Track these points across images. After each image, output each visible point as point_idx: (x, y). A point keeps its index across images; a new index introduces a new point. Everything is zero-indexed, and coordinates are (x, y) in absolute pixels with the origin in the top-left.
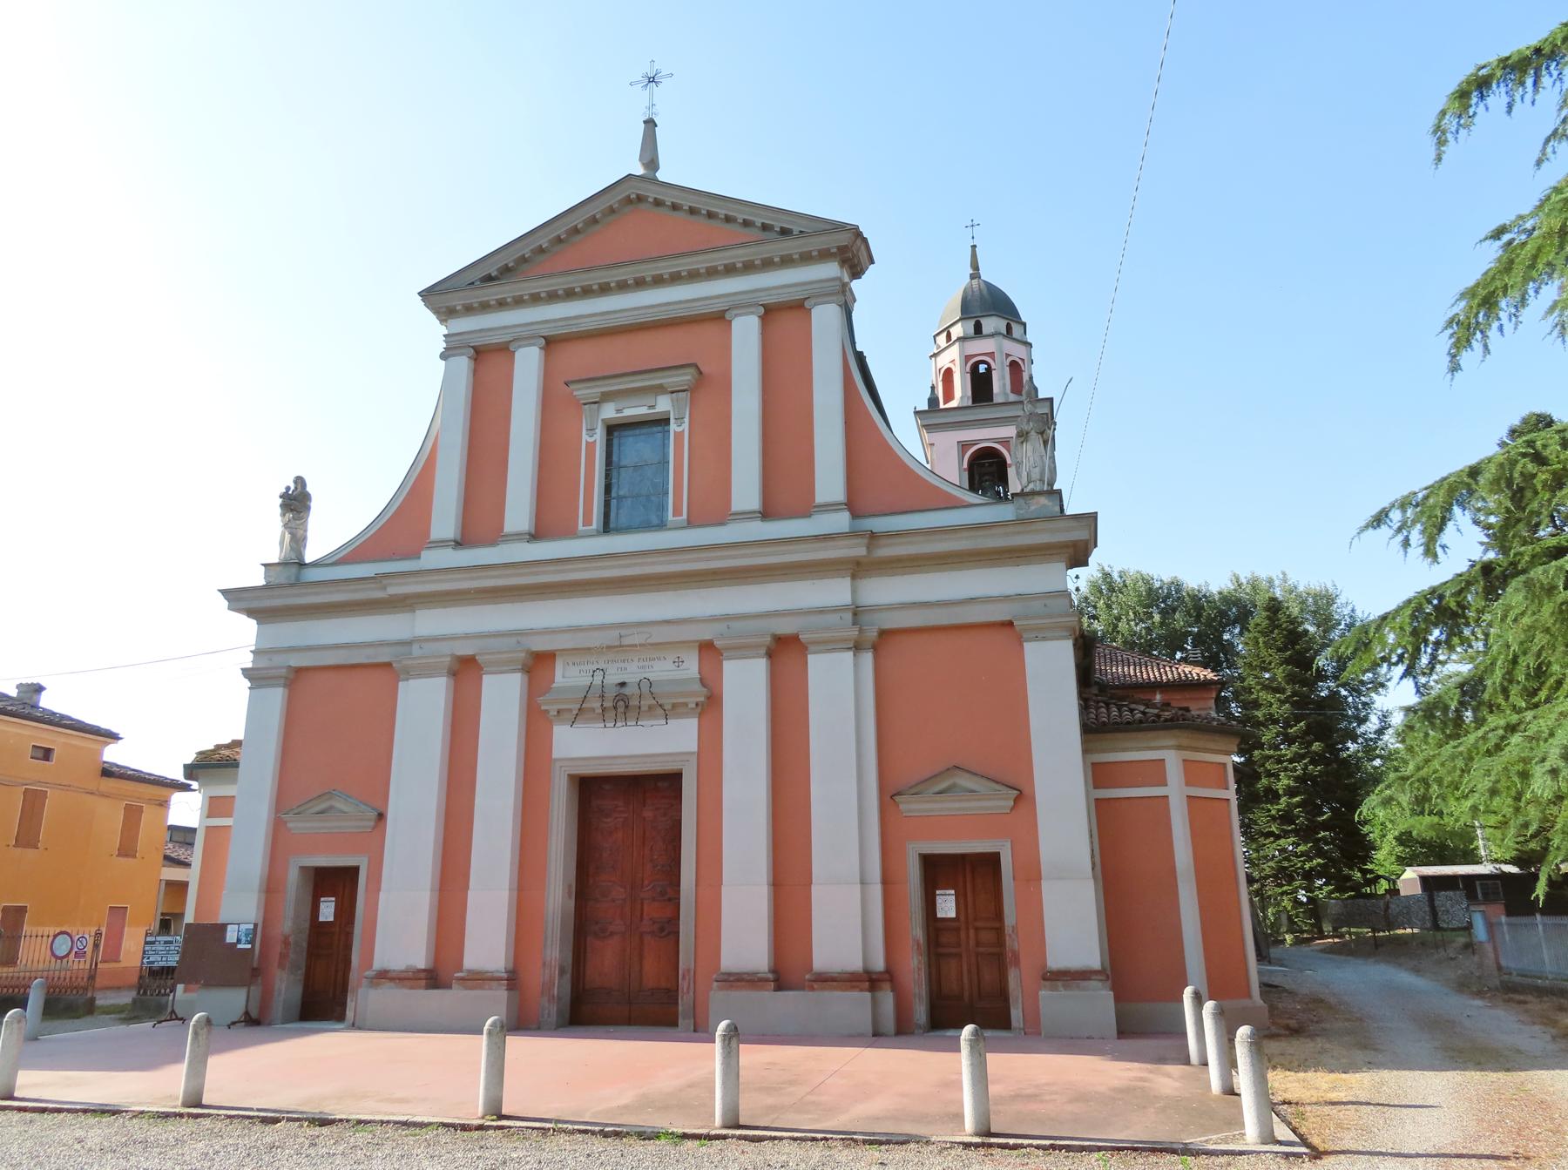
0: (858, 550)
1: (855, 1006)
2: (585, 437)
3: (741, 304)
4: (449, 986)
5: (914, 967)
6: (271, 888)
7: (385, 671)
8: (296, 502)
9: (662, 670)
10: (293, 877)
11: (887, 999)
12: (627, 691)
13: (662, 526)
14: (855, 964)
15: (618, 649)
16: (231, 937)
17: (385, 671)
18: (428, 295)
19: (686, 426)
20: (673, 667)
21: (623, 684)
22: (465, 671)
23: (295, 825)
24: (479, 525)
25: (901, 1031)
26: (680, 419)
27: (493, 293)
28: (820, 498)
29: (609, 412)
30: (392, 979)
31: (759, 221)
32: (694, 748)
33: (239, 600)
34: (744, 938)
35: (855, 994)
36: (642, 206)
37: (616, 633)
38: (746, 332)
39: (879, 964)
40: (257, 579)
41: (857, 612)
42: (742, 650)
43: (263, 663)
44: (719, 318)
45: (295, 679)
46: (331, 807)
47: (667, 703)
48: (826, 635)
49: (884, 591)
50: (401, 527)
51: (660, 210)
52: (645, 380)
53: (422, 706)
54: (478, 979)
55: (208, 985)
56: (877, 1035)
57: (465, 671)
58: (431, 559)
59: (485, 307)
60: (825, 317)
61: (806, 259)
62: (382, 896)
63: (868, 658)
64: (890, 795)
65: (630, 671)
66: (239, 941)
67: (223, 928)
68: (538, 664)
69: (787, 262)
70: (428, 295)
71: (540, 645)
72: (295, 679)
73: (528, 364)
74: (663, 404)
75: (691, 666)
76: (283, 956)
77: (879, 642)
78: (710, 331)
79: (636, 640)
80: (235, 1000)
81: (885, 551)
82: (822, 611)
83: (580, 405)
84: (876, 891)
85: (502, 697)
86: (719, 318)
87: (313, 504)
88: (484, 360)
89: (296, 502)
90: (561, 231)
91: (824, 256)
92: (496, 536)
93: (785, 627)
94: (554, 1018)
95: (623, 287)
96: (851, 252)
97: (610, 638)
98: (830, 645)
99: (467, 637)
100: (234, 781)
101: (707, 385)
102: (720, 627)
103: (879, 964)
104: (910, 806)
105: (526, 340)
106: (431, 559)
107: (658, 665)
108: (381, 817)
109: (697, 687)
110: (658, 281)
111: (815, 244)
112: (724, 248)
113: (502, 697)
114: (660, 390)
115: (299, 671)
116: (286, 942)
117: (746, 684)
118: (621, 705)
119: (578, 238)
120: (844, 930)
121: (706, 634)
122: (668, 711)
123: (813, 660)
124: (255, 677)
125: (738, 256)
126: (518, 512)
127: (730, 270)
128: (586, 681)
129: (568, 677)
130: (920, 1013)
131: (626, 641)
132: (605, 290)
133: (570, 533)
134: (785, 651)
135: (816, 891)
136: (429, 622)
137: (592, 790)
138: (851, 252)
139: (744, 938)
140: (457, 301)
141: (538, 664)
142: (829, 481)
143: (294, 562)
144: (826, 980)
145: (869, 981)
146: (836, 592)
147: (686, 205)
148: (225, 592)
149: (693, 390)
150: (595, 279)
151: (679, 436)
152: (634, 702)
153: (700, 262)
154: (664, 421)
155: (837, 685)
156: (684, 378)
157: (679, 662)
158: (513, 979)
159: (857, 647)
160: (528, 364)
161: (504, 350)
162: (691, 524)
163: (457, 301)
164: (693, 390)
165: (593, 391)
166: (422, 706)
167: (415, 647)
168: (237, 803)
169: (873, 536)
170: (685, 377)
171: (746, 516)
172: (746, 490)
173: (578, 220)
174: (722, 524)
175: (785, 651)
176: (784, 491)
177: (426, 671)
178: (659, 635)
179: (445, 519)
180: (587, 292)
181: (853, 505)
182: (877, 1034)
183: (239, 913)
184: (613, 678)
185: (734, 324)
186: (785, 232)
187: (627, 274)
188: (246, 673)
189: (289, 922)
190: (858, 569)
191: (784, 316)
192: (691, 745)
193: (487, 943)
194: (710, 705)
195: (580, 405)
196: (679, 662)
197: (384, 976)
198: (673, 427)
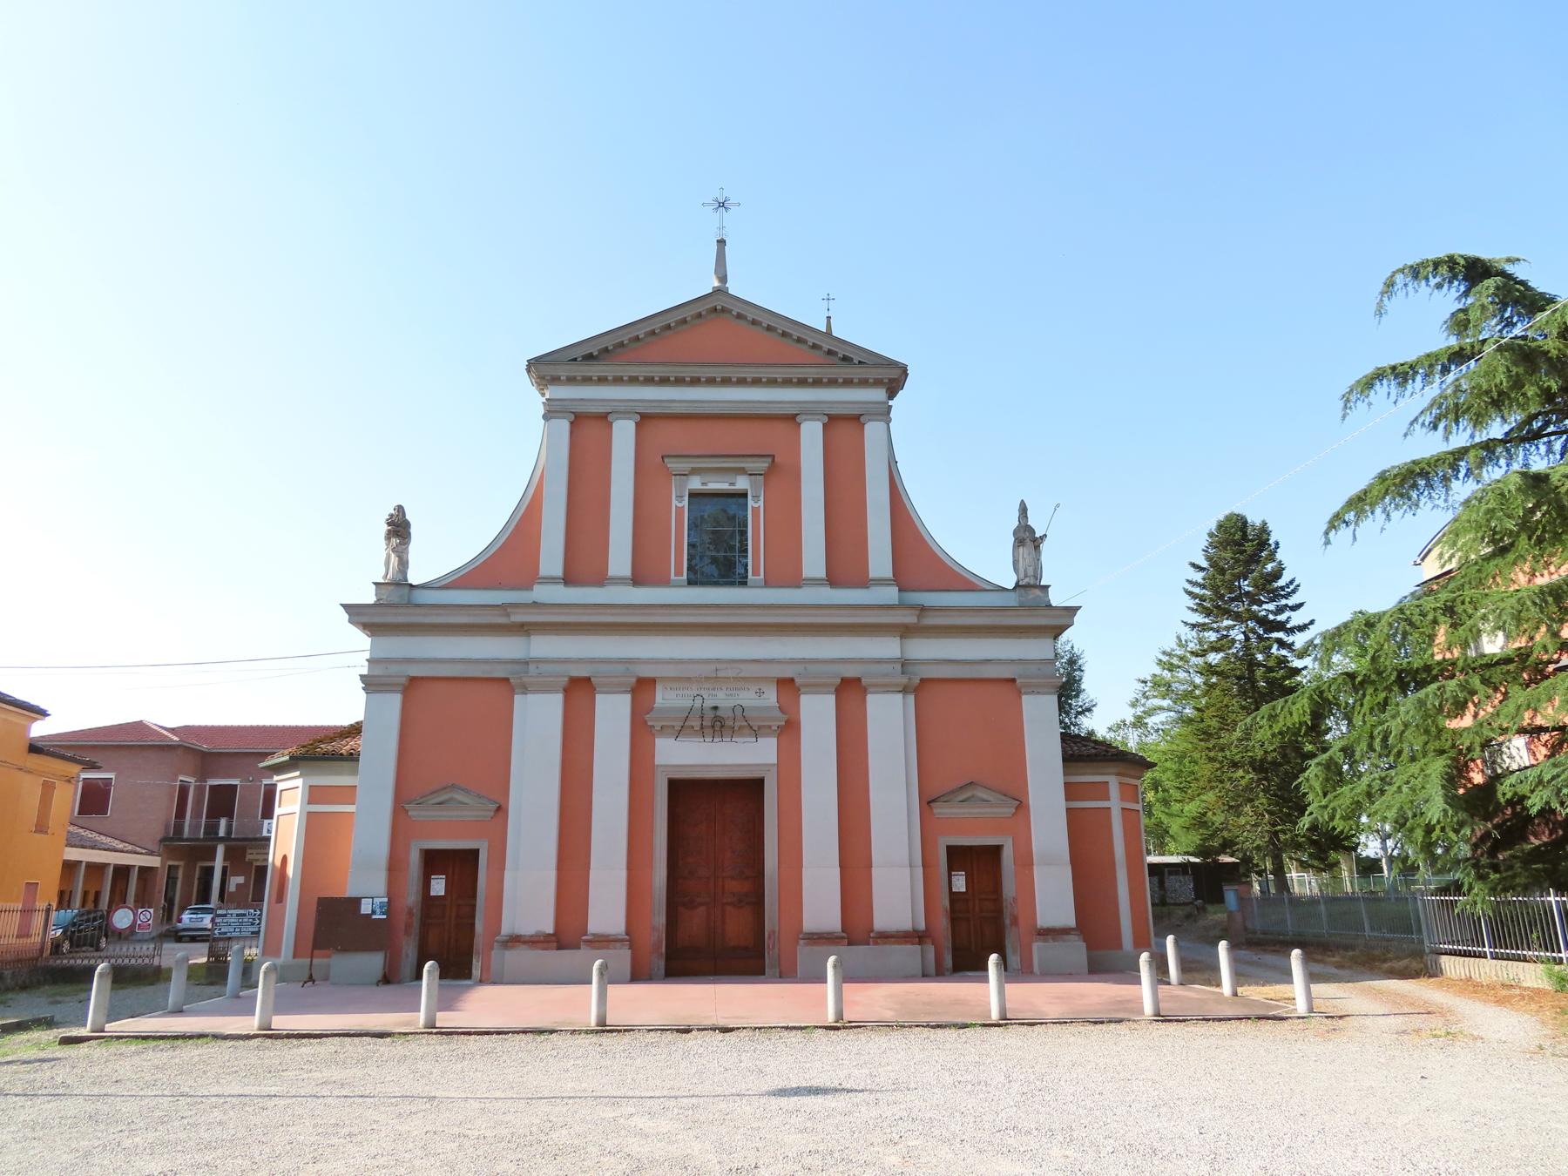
0: (910, 618)
1: (909, 955)
2: (675, 503)
3: (811, 411)
4: (578, 947)
5: (943, 924)
6: (395, 866)
7: (504, 685)
8: (399, 528)
9: (747, 698)
10: (415, 858)
11: (930, 950)
12: (719, 713)
13: (743, 582)
14: (906, 925)
15: (715, 680)
16: (366, 908)
17: (504, 685)
18: (535, 365)
19: (761, 503)
20: (754, 696)
21: (716, 708)
22: (579, 691)
23: (414, 812)
24: (583, 564)
25: (938, 973)
26: (756, 497)
27: (595, 370)
28: (872, 575)
29: (695, 483)
30: (525, 942)
31: (811, 341)
32: (775, 761)
33: (358, 614)
34: (821, 904)
35: (909, 947)
36: (727, 315)
37: (713, 667)
38: (811, 434)
39: (922, 926)
40: (369, 597)
41: (905, 664)
42: (816, 688)
43: (379, 671)
44: (791, 419)
45: (412, 687)
46: (451, 799)
47: (755, 724)
48: (886, 680)
49: (925, 649)
50: (509, 559)
51: (742, 322)
52: (732, 460)
53: (537, 721)
54: (603, 942)
55: (345, 950)
56: (925, 976)
57: (579, 691)
58: (541, 593)
59: (587, 380)
60: (872, 430)
61: (864, 383)
62: (508, 875)
63: (911, 698)
64: (928, 802)
65: (723, 698)
66: (374, 912)
67: (357, 901)
68: (642, 688)
69: (848, 383)
70: (535, 365)
71: (646, 672)
72: (412, 687)
73: (624, 434)
74: (742, 483)
75: (771, 697)
76: (408, 926)
77: (921, 688)
78: (781, 428)
79: (730, 673)
80: (374, 962)
81: (930, 620)
82: (879, 661)
83: (670, 474)
84: (919, 871)
85: (612, 715)
86: (791, 419)
87: (412, 530)
88: (584, 431)
89: (399, 528)
90: (657, 326)
91: (878, 383)
92: (600, 579)
93: (851, 672)
94: (663, 972)
95: (711, 382)
96: (893, 378)
97: (707, 670)
98: (886, 688)
99: (580, 661)
100: (355, 772)
101: (780, 472)
102: (800, 668)
103: (922, 926)
104: (940, 810)
105: (624, 414)
106: (541, 593)
107: (743, 694)
108: (501, 810)
109: (778, 713)
110: (742, 382)
111: (872, 374)
112: (804, 365)
113: (612, 715)
114: (742, 471)
115: (413, 680)
116: (410, 913)
117: (817, 713)
118: (717, 725)
119: (668, 333)
120: (898, 897)
121: (787, 672)
122: (756, 732)
123: (870, 698)
124: (371, 684)
125: (811, 373)
126: (620, 560)
127: (802, 383)
128: (689, 703)
129: (664, 698)
130: (948, 961)
131: (721, 674)
132: (695, 382)
133: (664, 582)
134: (850, 691)
135: (875, 872)
136: (544, 647)
137: (685, 792)
138: (893, 378)
139: (821, 904)
140: (550, 371)
141: (642, 688)
142: (880, 560)
143: (397, 587)
144: (886, 937)
145: (916, 937)
146: (888, 647)
147: (796, 334)
148: (346, 607)
149: (767, 475)
150: (687, 372)
151: (756, 511)
152: (729, 723)
153: (779, 374)
154: (744, 495)
155: (888, 716)
156: (763, 465)
157: (760, 693)
158: (631, 937)
159: (905, 690)
160: (624, 434)
161: (604, 419)
162: (767, 584)
163: (550, 371)
164: (767, 475)
165: (685, 465)
166: (537, 721)
167: (532, 667)
168: (359, 793)
169: (923, 609)
170: (763, 465)
171: (814, 582)
172: (814, 560)
173: (672, 320)
174: (799, 587)
175: (850, 691)
176: (845, 566)
177: (545, 689)
178: (749, 670)
179: (551, 560)
180: (679, 382)
181: (900, 579)
182: (924, 975)
183: (367, 885)
184: (709, 703)
185: (803, 426)
186: (845, 359)
187: (718, 373)
188: (362, 677)
189: (412, 897)
190: (905, 632)
191: (844, 427)
192: (772, 758)
193: (607, 909)
194: (789, 730)
195: (670, 474)
196: (760, 693)
197: (515, 940)
198: (751, 503)
